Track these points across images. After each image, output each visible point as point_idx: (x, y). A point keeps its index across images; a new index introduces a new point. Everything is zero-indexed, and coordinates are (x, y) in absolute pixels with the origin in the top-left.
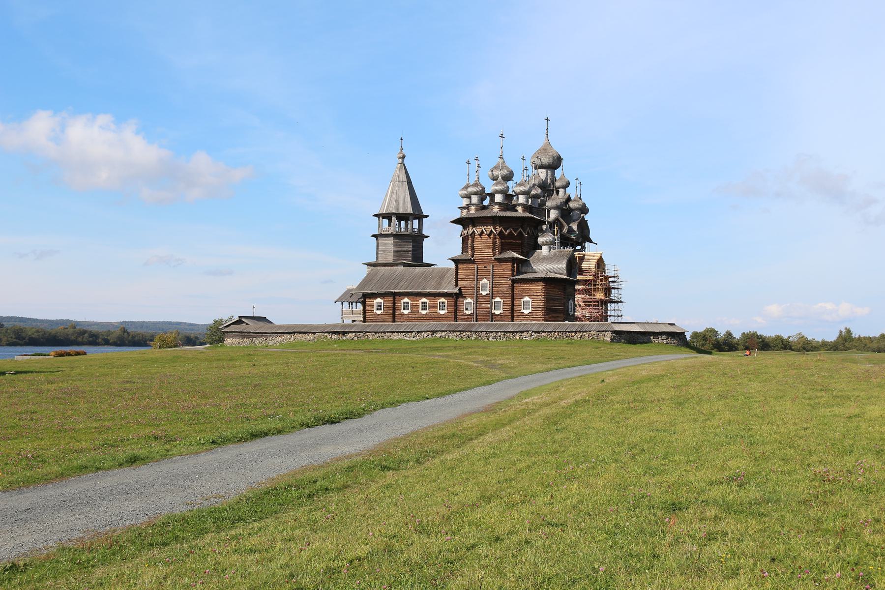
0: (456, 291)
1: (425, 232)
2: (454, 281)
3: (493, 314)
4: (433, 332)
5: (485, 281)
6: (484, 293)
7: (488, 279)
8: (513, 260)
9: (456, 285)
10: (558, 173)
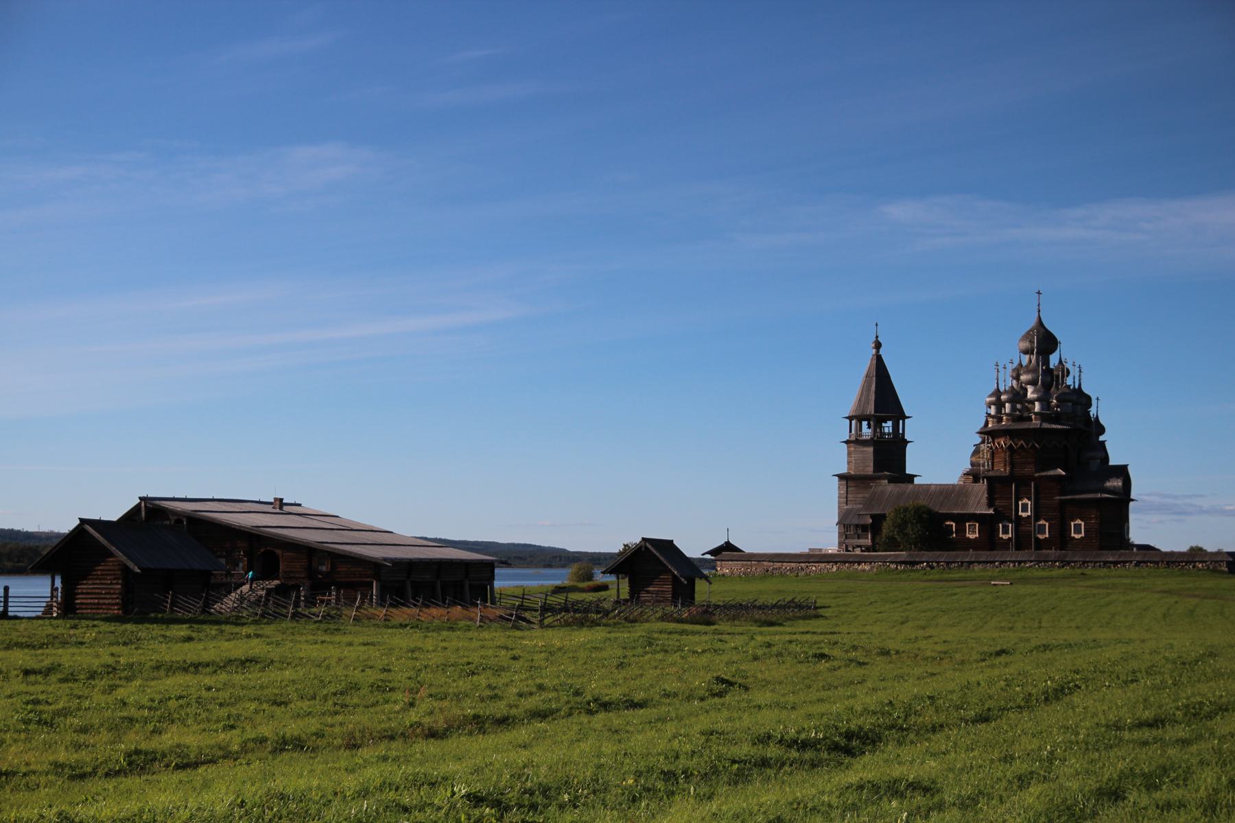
0: (991, 511)
2: (984, 500)
3: (1037, 539)
4: (1020, 562)
5: (1026, 501)
6: (1024, 515)
7: (1029, 499)
8: (1060, 476)
9: (990, 505)
10: (1054, 360)
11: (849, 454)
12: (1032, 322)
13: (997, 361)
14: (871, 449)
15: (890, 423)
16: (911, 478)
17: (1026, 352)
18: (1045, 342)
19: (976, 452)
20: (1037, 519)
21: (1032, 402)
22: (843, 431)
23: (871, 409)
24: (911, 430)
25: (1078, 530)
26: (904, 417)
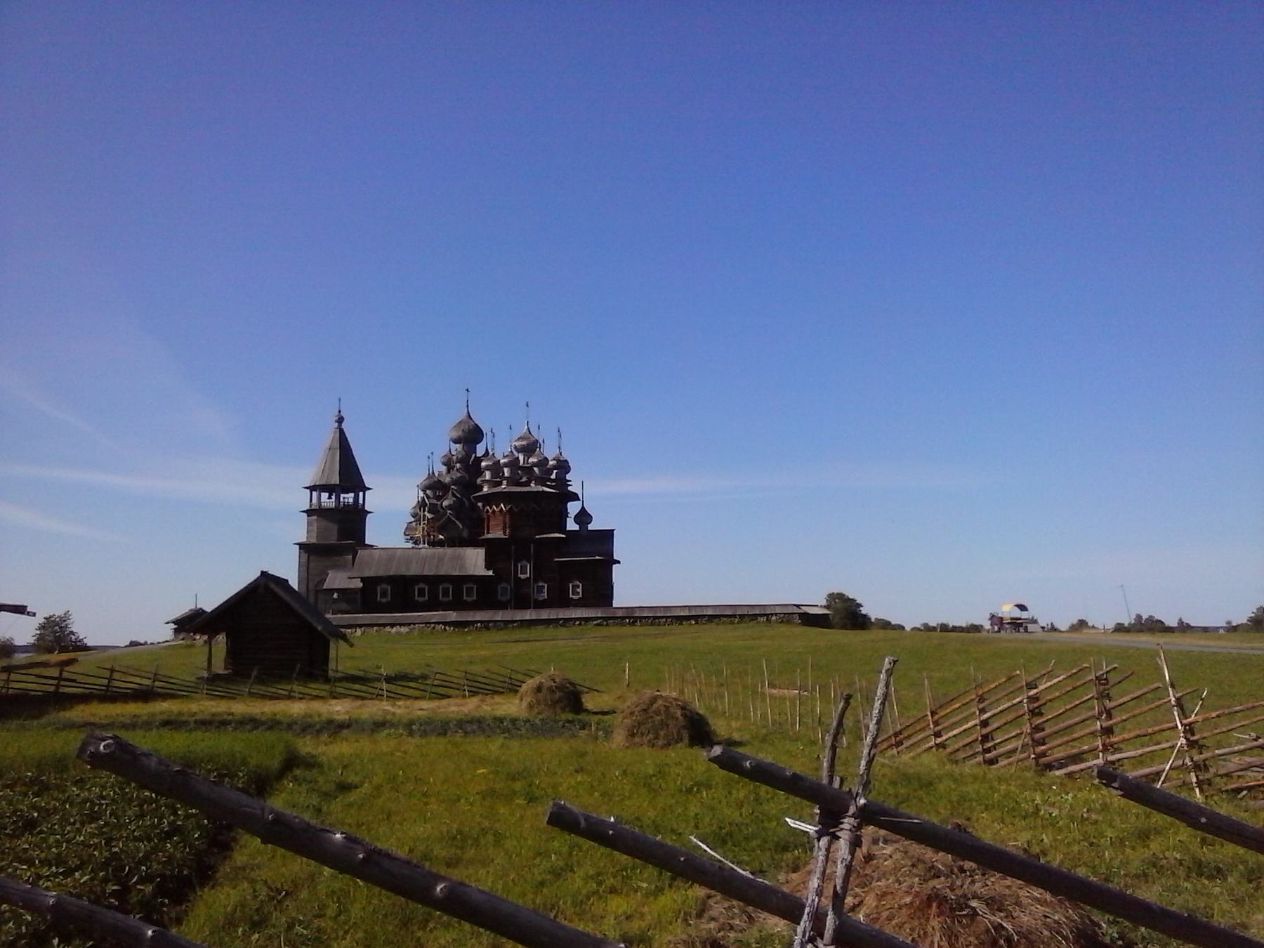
0: (491, 573)
6: (523, 577)
9: (488, 567)
13: (433, 450)
15: (352, 495)
17: (456, 441)
20: (536, 581)
22: (304, 500)
23: (336, 480)
24: (371, 501)
25: (577, 590)
26: (365, 489)
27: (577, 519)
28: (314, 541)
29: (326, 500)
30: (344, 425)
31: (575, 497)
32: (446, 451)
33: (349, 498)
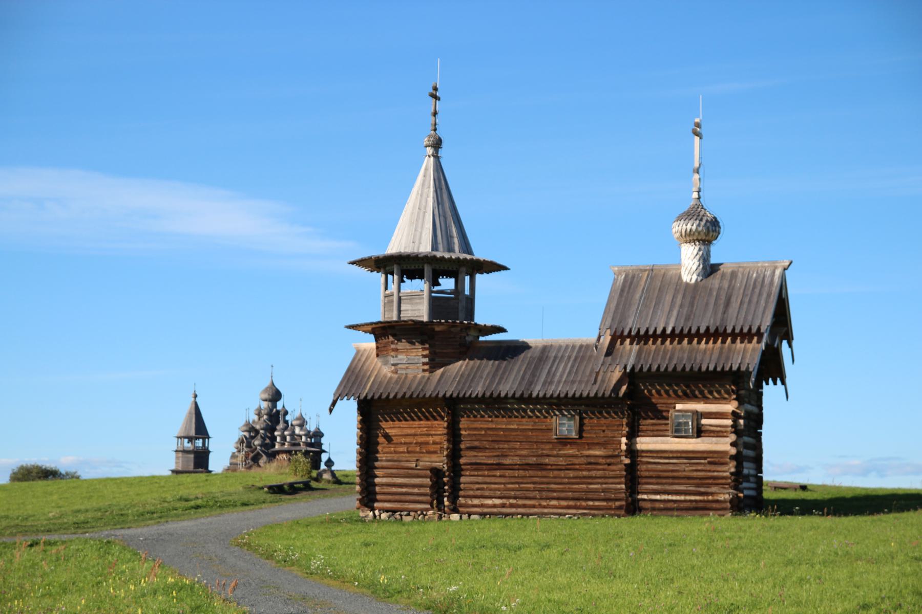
1: (210, 449)
10: (279, 406)
11: (177, 458)
12: (267, 383)
14: (192, 456)
15: (201, 440)
16: (210, 472)
18: (275, 396)
19: (233, 456)
21: (300, 436)
22: (174, 445)
24: (212, 445)
26: (209, 438)
27: (326, 464)
28: (180, 469)
29: (187, 445)
30: (197, 400)
31: (324, 451)
32: (257, 406)
33: (199, 443)
